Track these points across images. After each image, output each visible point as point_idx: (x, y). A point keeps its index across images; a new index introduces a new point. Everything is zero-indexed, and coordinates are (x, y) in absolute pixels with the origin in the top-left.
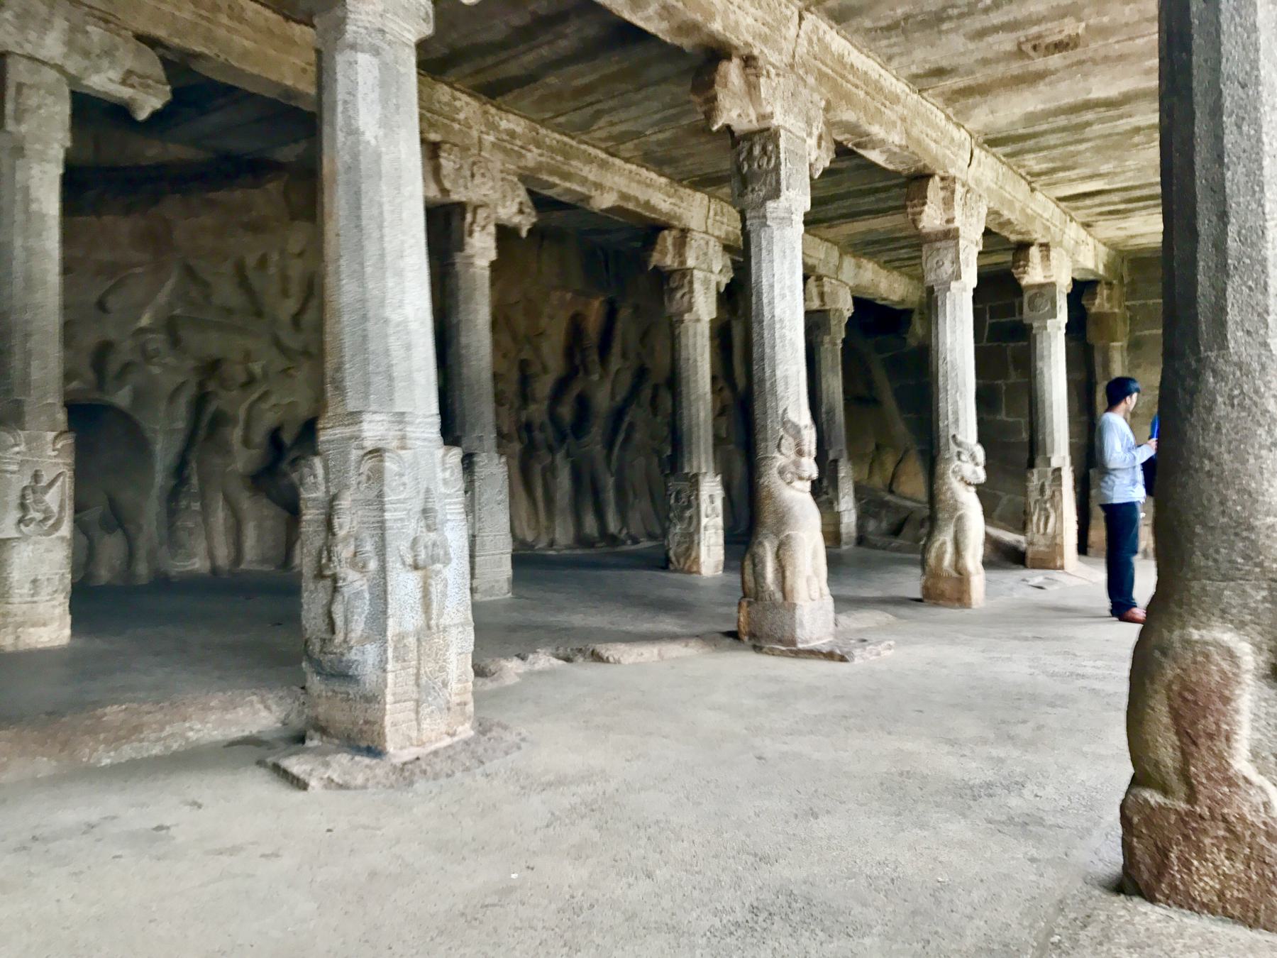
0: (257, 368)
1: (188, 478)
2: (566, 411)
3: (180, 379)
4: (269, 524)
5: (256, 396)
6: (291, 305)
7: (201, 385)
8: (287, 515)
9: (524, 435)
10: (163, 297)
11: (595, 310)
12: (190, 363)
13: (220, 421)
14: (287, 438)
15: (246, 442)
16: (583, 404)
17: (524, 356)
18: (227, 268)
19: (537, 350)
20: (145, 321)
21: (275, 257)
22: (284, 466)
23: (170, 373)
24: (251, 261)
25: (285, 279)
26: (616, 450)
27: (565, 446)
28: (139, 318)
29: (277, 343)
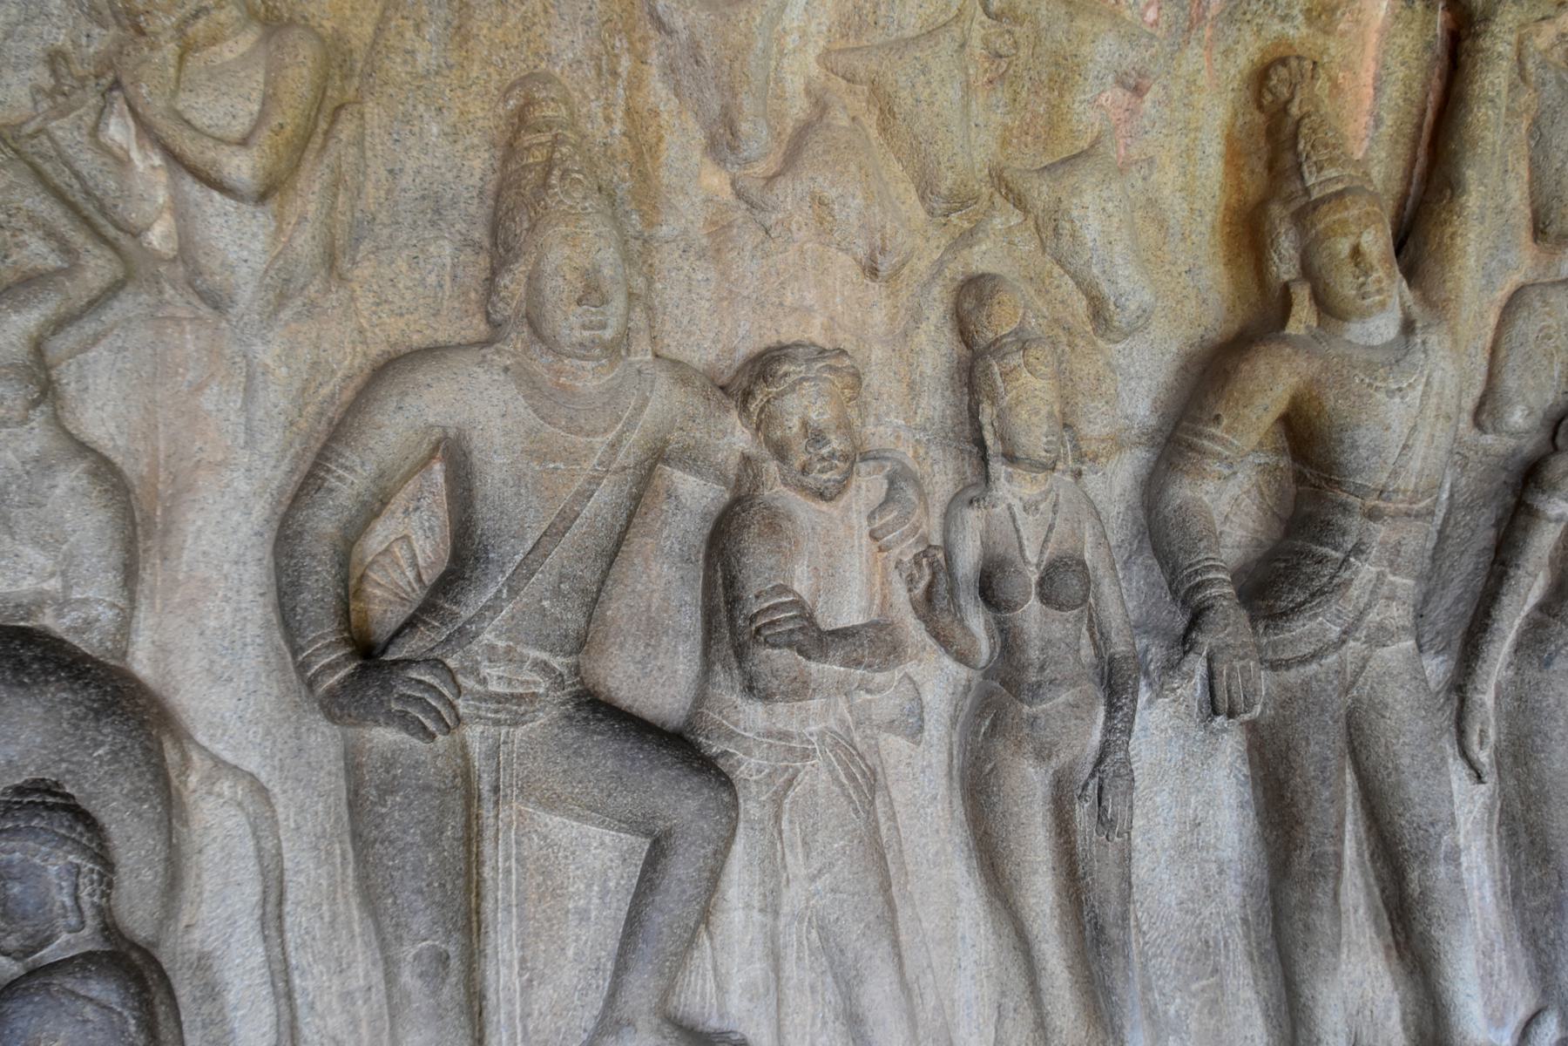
9: (977, 621)
17: (982, 258)
19: (1051, 228)
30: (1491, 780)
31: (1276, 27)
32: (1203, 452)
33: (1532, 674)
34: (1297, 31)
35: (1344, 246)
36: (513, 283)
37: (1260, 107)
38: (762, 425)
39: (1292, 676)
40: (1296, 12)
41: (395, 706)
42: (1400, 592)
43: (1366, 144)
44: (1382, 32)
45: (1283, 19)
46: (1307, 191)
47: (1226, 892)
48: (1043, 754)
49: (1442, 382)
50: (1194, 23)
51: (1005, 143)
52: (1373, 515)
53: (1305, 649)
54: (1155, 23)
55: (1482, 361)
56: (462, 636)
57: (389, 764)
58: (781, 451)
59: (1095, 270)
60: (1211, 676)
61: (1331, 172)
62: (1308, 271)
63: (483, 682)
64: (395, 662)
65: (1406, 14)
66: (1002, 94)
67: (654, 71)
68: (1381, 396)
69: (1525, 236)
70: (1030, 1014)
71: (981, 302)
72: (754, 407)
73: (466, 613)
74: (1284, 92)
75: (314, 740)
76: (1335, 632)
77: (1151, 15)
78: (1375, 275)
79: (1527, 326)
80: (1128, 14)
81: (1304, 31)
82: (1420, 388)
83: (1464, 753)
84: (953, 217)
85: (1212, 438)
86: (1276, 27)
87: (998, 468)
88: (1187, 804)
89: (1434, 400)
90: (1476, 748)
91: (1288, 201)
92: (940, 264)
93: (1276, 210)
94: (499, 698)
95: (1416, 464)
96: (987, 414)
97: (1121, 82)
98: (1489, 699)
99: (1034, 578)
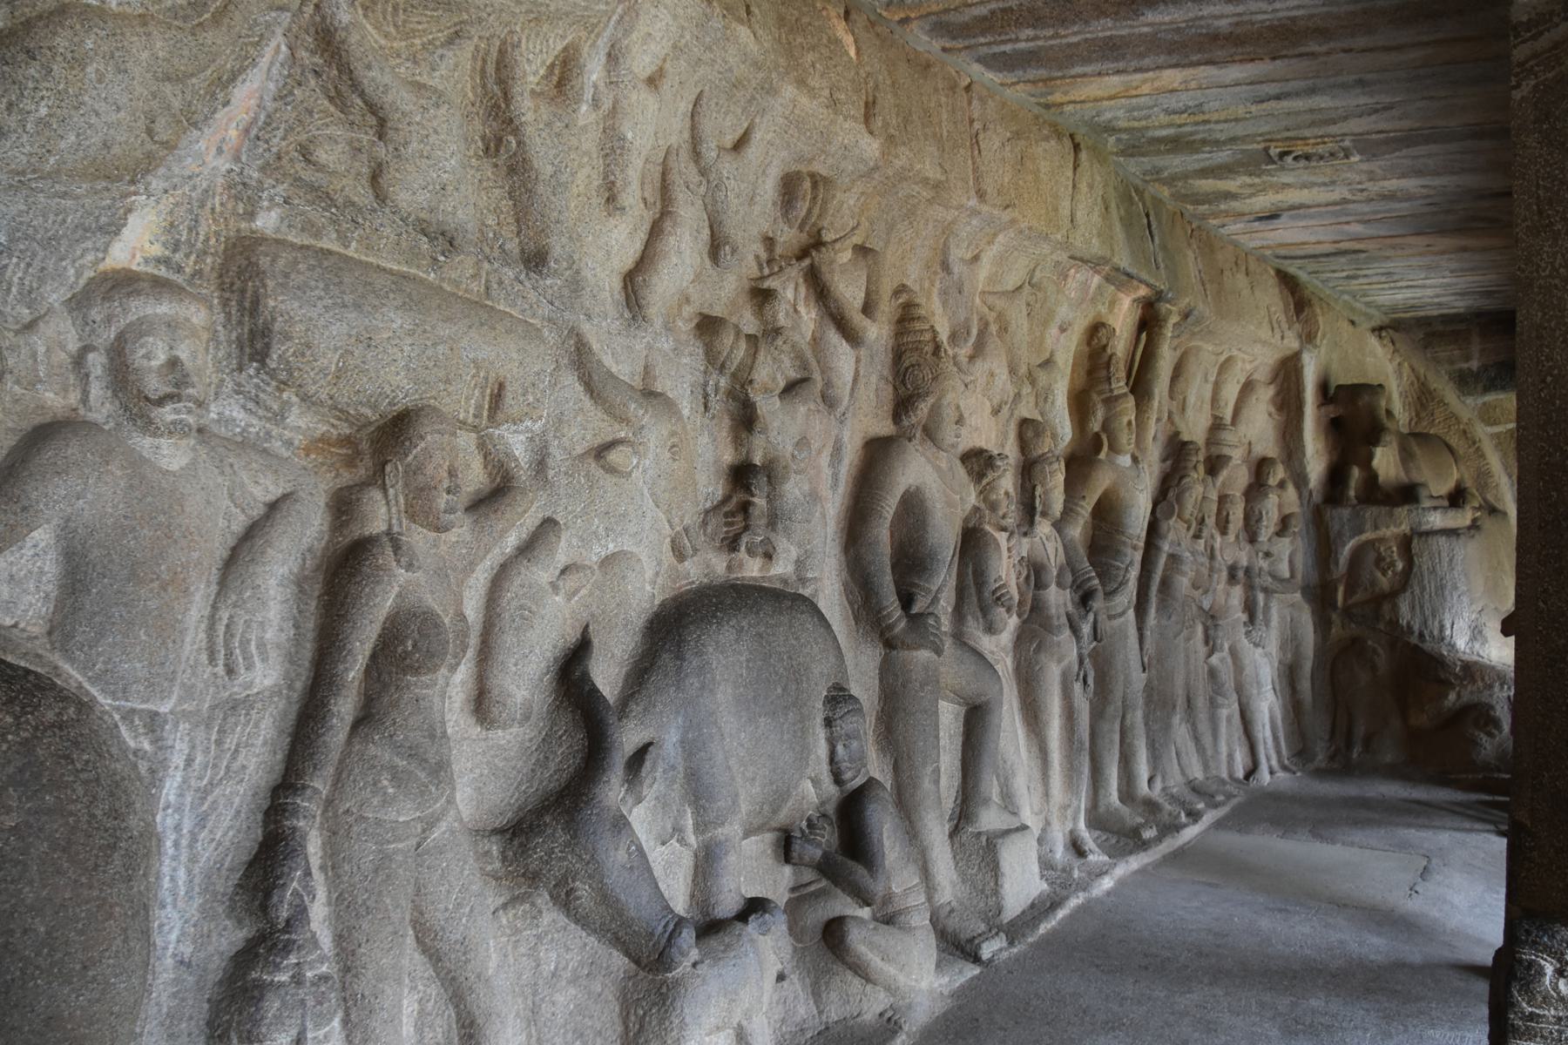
0: (516, 443)
1: (300, 913)
2: (1077, 531)
3: (265, 489)
4: (564, 998)
5: (512, 540)
6: (619, 241)
7: (343, 506)
8: (619, 961)
10: (211, 152)
11: (1122, 316)
12: (301, 422)
13: (404, 650)
14: (606, 675)
15: (482, 704)
16: (1107, 515)
18: (455, 72)
20: (137, 243)
21: (594, 72)
22: (612, 790)
23: (220, 469)
24: (532, 69)
25: (613, 147)
26: (1152, 612)
27: (1091, 617)
28: (113, 229)
29: (581, 357)
32: (1078, 514)
33: (1164, 622)
34: (1103, 310)
35: (1125, 420)
36: (924, 408)
37: (1089, 344)
38: (984, 493)
46: (1111, 391)
48: (1059, 661)
53: (1120, 610)
56: (935, 600)
57: (926, 668)
58: (993, 507)
62: (1106, 426)
64: (921, 615)
67: (935, 291)
70: (1040, 789)
71: (1038, 435)
72: (985, 482)
73: (934, 588)
74: (1104, 341)
75: (863, 659)
87: (1037, 518)
91: (1100, 393)
93: (1095, 397)
96: (1039, 491)
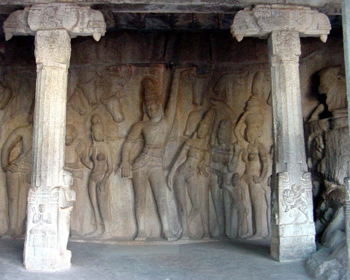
30: (172, 190)
31: (145, 75)
39: (135, 171)
40: (147, 72)
41: (10, 169)
42: (154, 160)
43: (162, 91)
44: (163, 74)
45: (146, 73)
47: (130, 205)
49: (164, 128)
50: (131, 75)
51: (102, 95)
52: (149, 148)
53: (137, 168)
54: (125, 76)
55: (185, 124)
59: (112, 113)
60: (122, 171)
61: (148, 96)
63: (21, 167)
65: (167, 71)
66: (102, 88)
68: (152, 130)
69: (192, 103)
76: (141, 165)
77: (124, 75)
78: (153, 112)
79: (191, 118)
80: (120, 75)
81: (149, 74)
82: (159, 129)
83: (168, 186)
84: (94, 106)
85: (130, 137)
86: (145, 75)
87: (94, 141)
88: (123, 191)
89: (161, 131)
90: (170, 185)
92: (90, 113)
94: (23, 169)
95: (156, 140)
97: (119, 84)
98: (172, 178)
99: (96, 156)
